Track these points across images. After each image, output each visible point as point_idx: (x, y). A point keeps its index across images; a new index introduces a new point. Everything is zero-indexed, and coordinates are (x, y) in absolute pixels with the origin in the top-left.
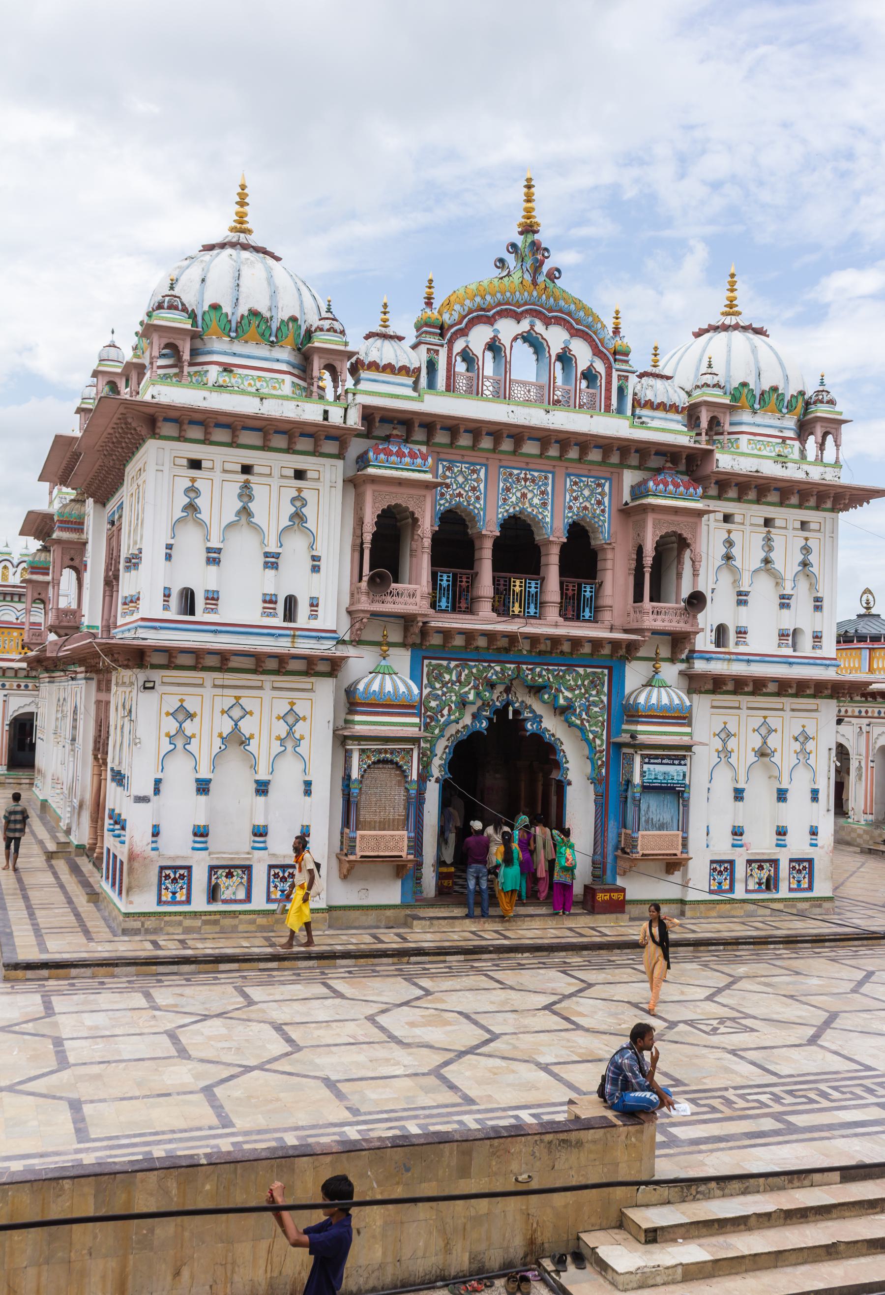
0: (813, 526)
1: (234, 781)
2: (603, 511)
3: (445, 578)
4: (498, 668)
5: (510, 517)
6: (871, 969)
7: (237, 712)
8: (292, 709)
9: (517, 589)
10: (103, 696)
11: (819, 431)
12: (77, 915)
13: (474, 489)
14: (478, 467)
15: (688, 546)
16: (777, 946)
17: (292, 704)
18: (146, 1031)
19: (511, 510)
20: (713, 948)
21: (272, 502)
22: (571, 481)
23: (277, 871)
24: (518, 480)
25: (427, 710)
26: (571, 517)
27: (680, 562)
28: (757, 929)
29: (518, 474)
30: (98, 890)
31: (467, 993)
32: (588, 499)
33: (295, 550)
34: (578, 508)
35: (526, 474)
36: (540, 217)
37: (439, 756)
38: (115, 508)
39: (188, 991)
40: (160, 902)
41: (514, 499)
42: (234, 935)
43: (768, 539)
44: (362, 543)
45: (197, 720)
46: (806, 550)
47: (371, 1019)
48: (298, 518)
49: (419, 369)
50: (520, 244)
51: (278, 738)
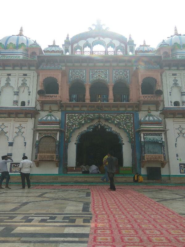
2: (127, 77)
17: (21, 125)
19: (95, 79)
21: (15, 82)
25: (67, 126)
41: (95, 76)
48: (24, 84)
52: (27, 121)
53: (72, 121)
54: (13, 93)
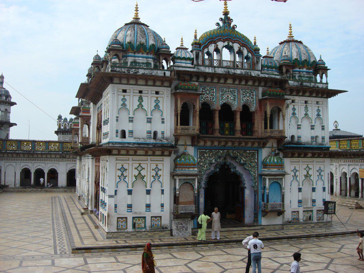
0: (320, 103)
1: (140, 190)
2: (253, 100)
3: (204, 123)
4: (222, 152)
5: (224, 103)
6: (343, 244)
7: (140, 168)
8: (157, 167)
9: (227, 126)
10: (97, 164)
11: (321, 72)
12: (92, 233)
13: (212, 95)
14: (213, 88)
15: (281, 110)
16: (314, 238)
17: (157, 165)
18: (116, 269)
19: (224, 101)
20: (293, 239)
21: (148, 103)
22: (243, 91)
23: (154, 218)
24: (226, 92)
26: (243, 103)
27: (279, 116)
28: (307, 233)
29: (226, 90)
30: (98, 225)
31: (216, 256)
32: (249, 97)
33: (157, 116)
34: (245, 100)
35: (228, 90)
36: (229, 9)
37: (204, 180)
38: (100, 105)
39: (128, 257)
40: (118, 229)
41: (225, 98)
42: (141, 239)
43: (306, 108)
44: (177, 114)
45: (127, 171)
46: (318, 110)
47: (186, 265)
48: (157, 106)
49: (193, 59)
50: (223, 18)
51: (153, 176)
52: (163, 160)
53: (203, 160)
54: (146, 120)
